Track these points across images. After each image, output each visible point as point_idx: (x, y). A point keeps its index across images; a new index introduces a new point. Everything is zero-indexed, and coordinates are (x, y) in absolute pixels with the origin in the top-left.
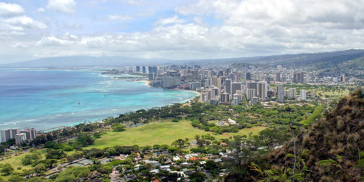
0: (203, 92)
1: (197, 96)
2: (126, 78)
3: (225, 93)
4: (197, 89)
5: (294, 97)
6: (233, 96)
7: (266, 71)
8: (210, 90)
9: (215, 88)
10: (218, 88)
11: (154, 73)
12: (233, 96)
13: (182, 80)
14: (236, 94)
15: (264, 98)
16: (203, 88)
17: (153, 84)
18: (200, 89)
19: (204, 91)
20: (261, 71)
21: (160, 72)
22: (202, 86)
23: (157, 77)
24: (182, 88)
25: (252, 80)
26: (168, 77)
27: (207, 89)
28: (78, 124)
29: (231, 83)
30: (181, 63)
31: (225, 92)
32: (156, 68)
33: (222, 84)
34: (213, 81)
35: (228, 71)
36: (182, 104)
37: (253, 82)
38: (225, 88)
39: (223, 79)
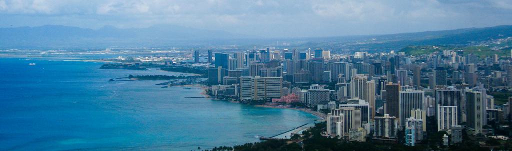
0: (333, 114)
1: (318, 122)
2: (155, 78)
3: (386, 116)
4: (320, 107)
8: (350, 107)
9: (362, 103)
10: (367, 104)
11: (221, 67)
12: (403, 123)
13: (284, 85)
14: (412, 118)
15: (479, 128)
16: (334, 102)
17: (219, 92)
18: (326, 106)
19: (336, 111)
20: (471, 64)
21: (236, 63)
22: (332, 100)
23: (228, 77)
24: (284, 103)
25: (449, 84)
26: (252, 77)
27: (341, 106)
29: (401, 92)
30: (284, 44)
31: (385, 115)
32: (226, 56)
33: (379, 94)
34: (356, 88)
35: (394, 62)
37: (452, 88)
38: (385, 105)
39: (380, 82)
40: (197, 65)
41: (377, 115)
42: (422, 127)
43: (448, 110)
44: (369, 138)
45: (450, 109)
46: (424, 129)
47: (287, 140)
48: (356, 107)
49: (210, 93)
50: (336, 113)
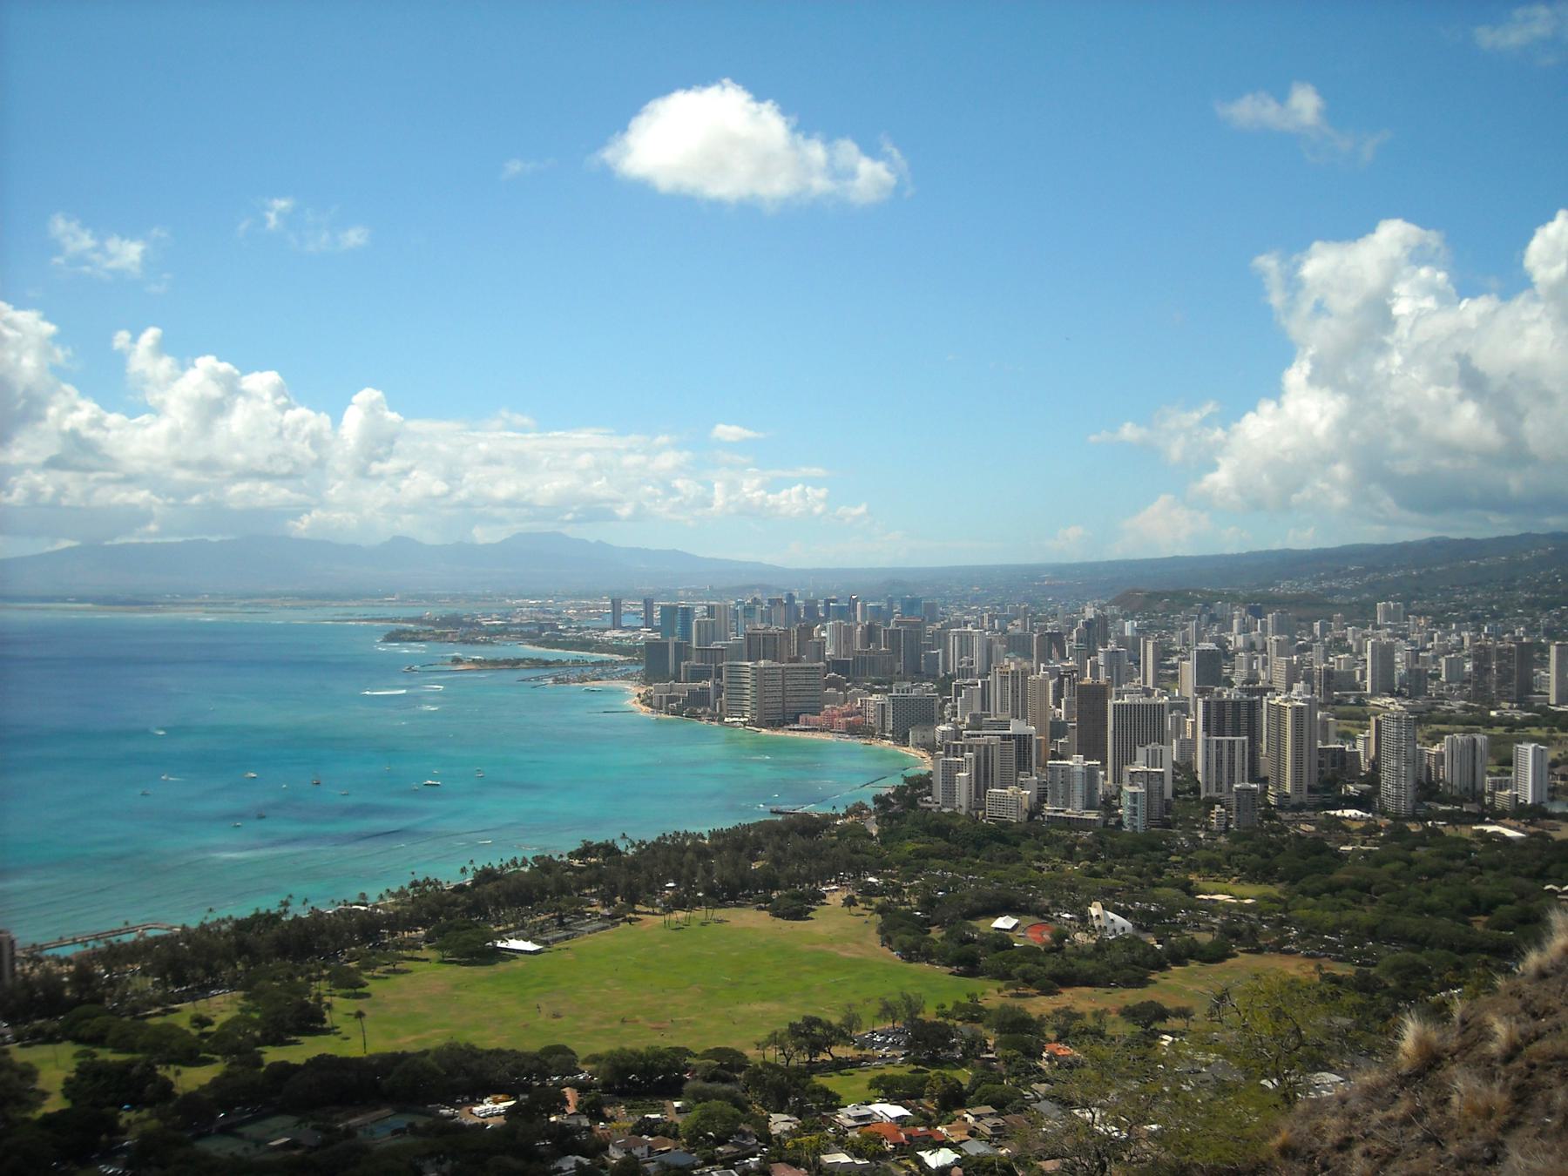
2: (514, 664)
3: (1076, 762)
5: (1478, 787)
6: (1118, 779)
7: (1311, 632)
8: (990, 737)
9: (1016, 727)
12: (1118, 779)
23: (693, 663)
25: (1231, 685)
28: (244, 911)
36: (826, 817)
39: (1061, 678)
40: (616, 633)
41: (1055, 756)
42: (1162, 788)
43: (1226, 746)
44: (1035, 811)
45: (1232, 743)
46: (1168, 794)
47: (837, 816)
48: (1004, 737)
49: (647, 701)
50: (955, 750)
